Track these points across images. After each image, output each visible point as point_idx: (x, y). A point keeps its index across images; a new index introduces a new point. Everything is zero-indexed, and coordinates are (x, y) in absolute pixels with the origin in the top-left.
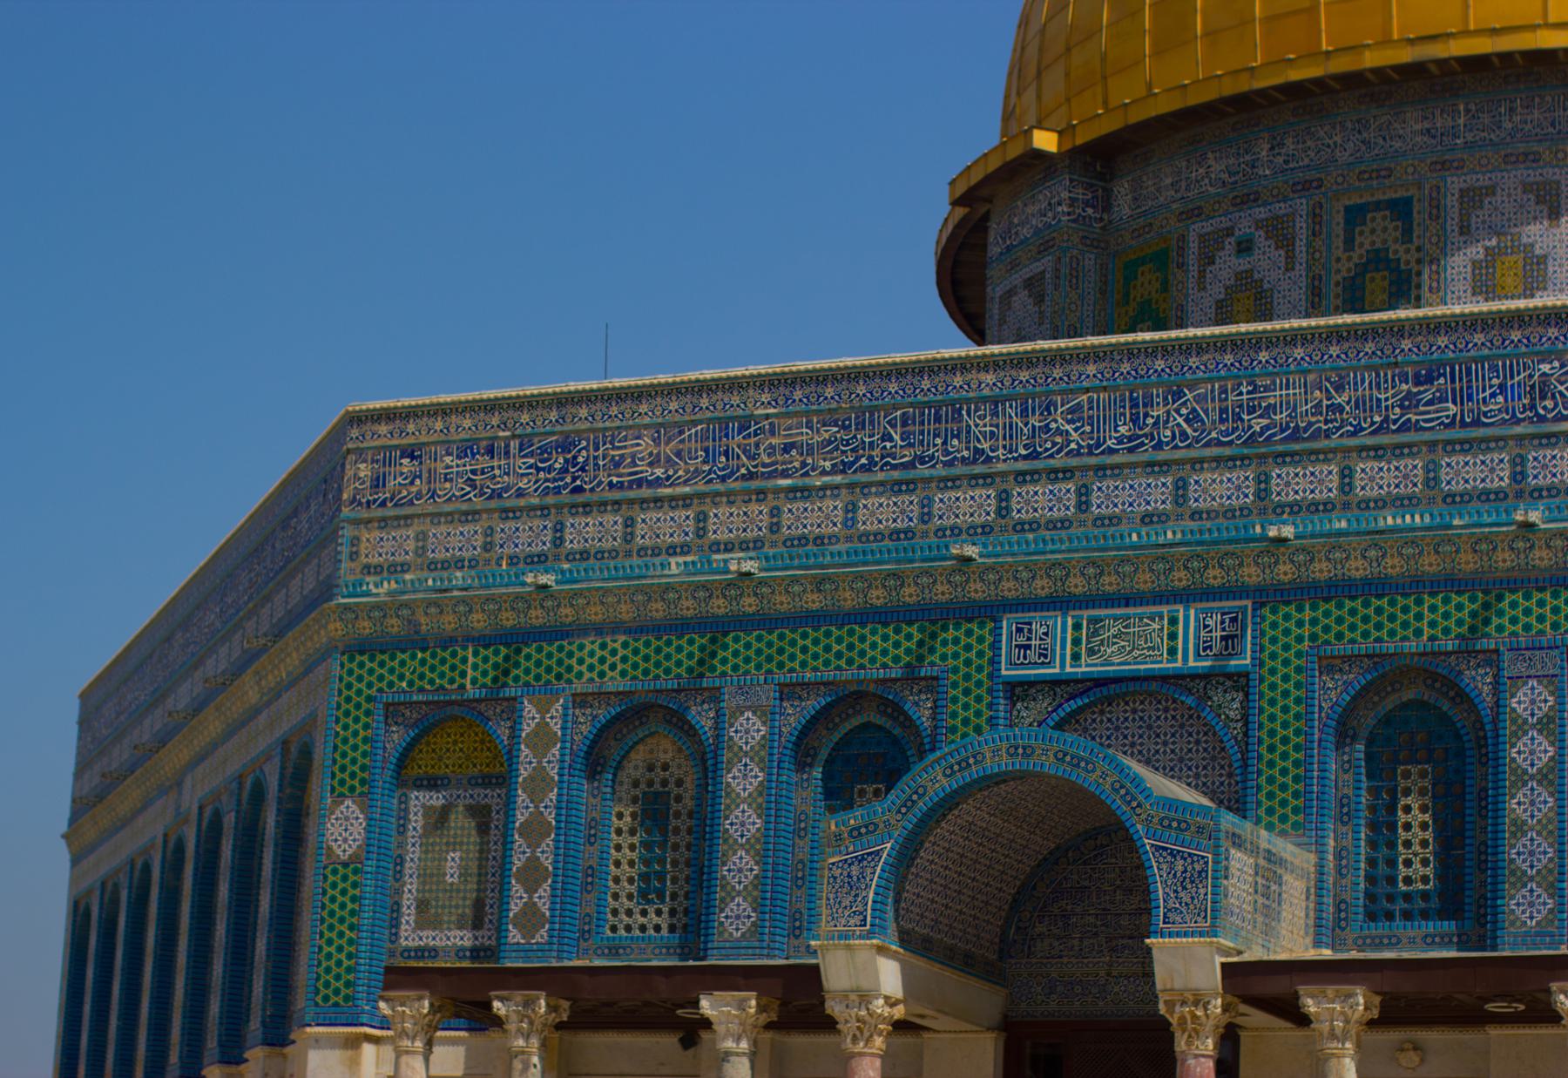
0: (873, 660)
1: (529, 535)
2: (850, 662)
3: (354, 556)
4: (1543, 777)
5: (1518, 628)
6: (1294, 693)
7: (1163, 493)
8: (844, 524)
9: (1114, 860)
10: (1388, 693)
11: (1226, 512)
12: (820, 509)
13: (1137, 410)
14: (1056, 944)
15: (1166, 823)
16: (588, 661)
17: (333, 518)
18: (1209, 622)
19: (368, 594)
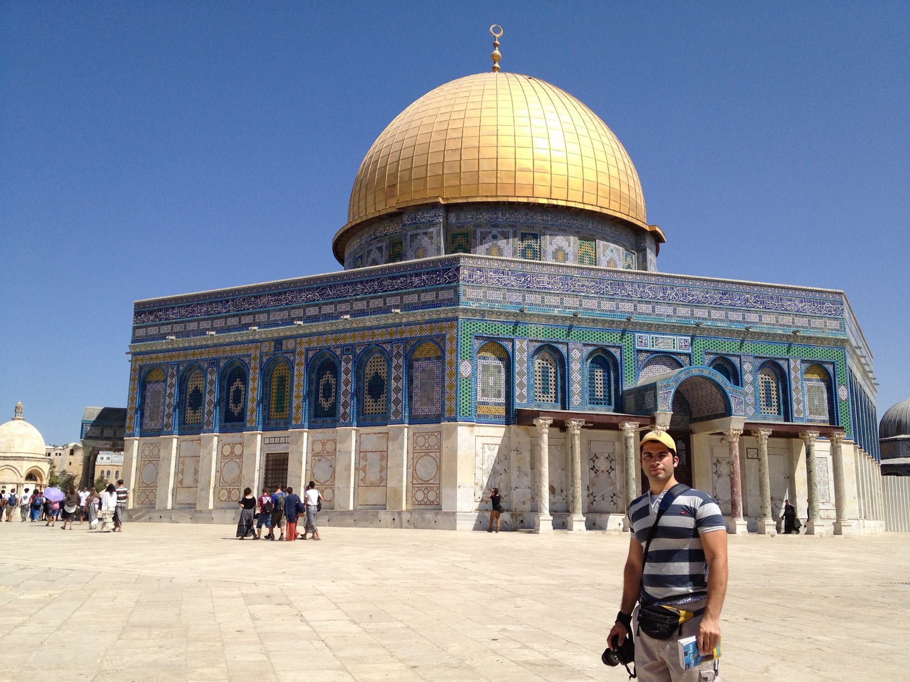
0: (606, 341)
1: (516, 297)
2: (600, 340)
3: (465, 295)
4: (751, 383)
6: (701, 360)
13: (664, 290)
16: (533, 332)
17: (449, 283)
19: (470, 306)
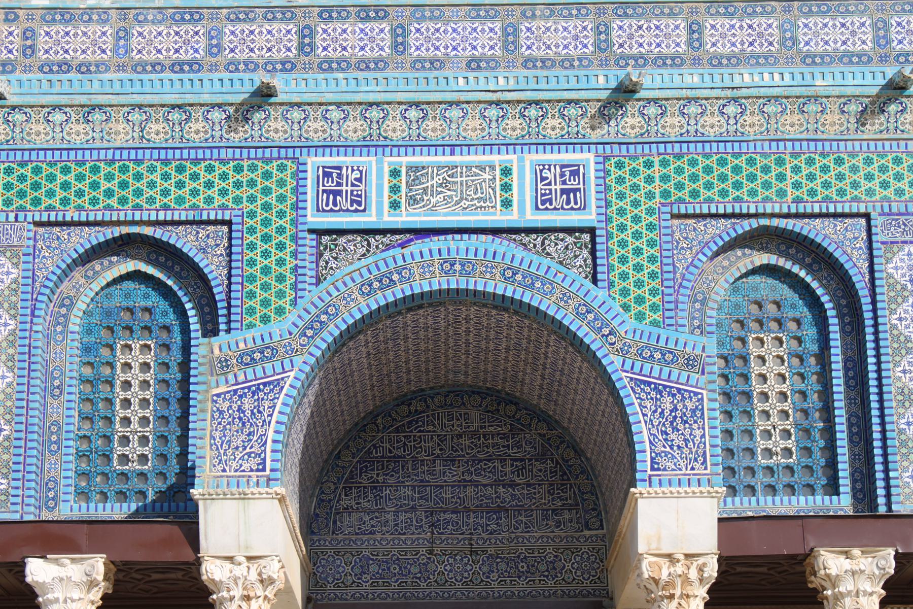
0: (151, 200)
2: (123, 201)
5: (890, 193)
6: (648, 252)
7: (491, 39)
8: (115, 51)
9: (431, 428)
10: (738, 258)
11: (563, 61)
12: (85, 34)
14: (367, 518)
15: (646, 354)
18: (546, 173)
